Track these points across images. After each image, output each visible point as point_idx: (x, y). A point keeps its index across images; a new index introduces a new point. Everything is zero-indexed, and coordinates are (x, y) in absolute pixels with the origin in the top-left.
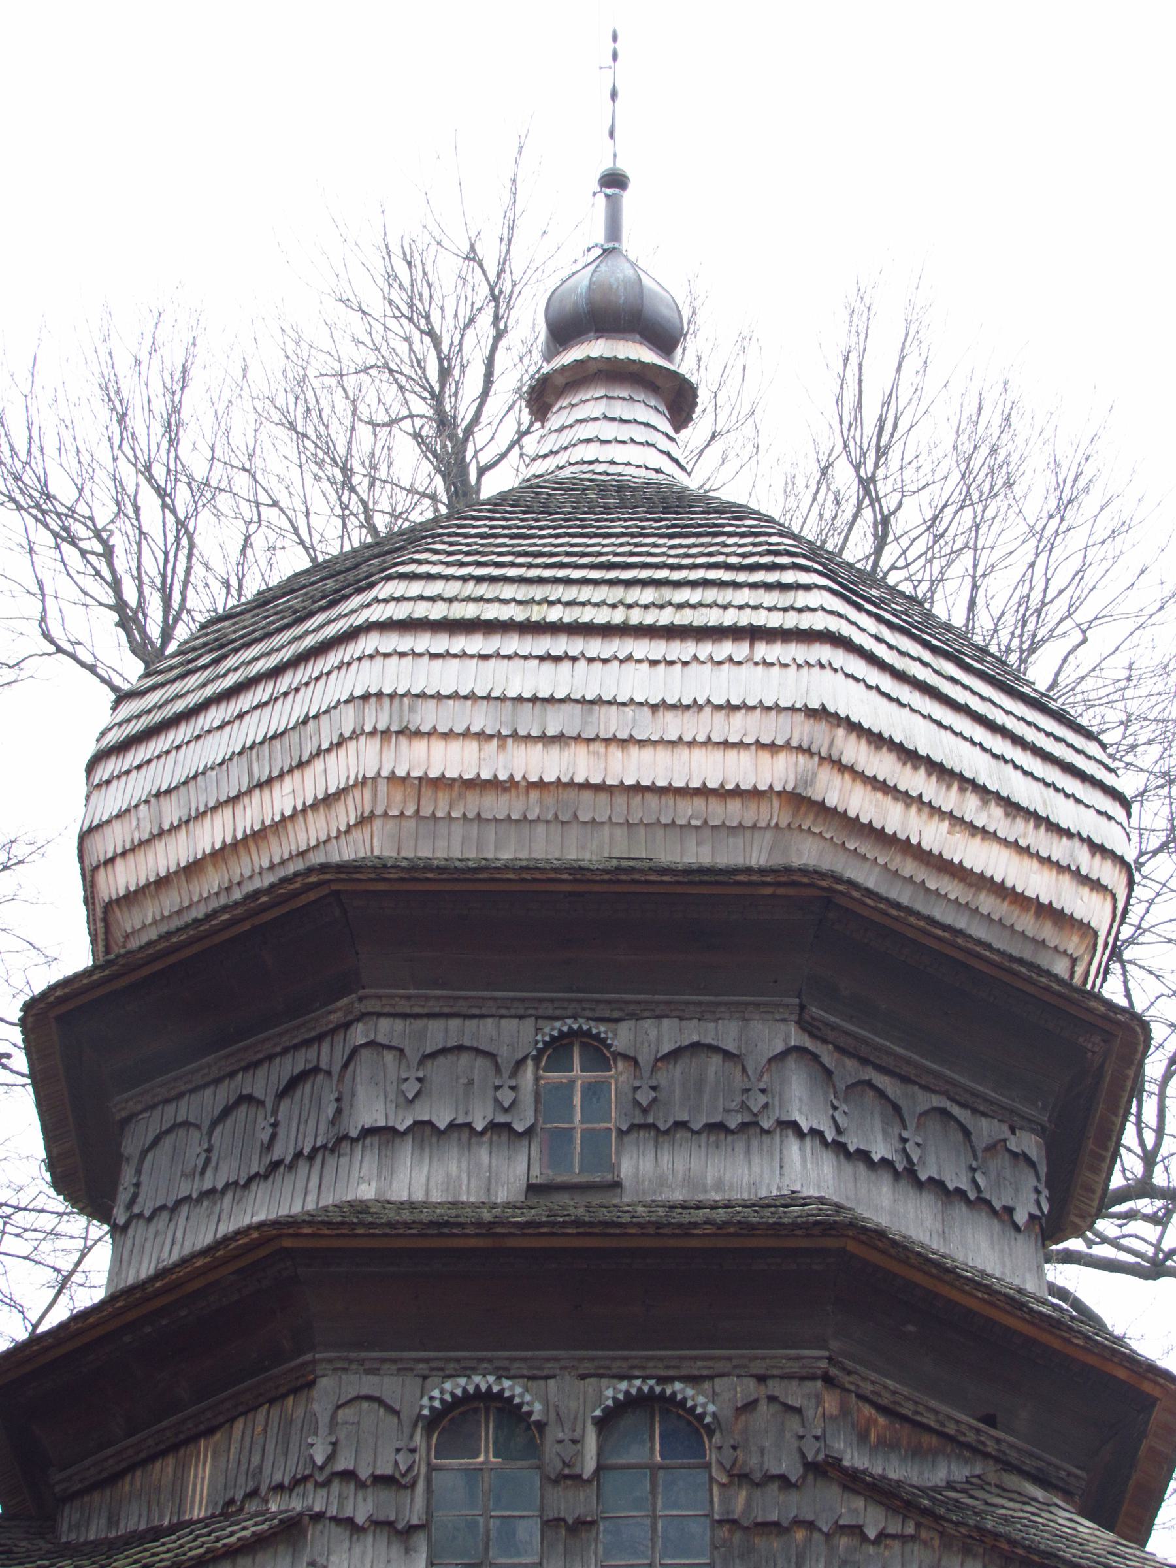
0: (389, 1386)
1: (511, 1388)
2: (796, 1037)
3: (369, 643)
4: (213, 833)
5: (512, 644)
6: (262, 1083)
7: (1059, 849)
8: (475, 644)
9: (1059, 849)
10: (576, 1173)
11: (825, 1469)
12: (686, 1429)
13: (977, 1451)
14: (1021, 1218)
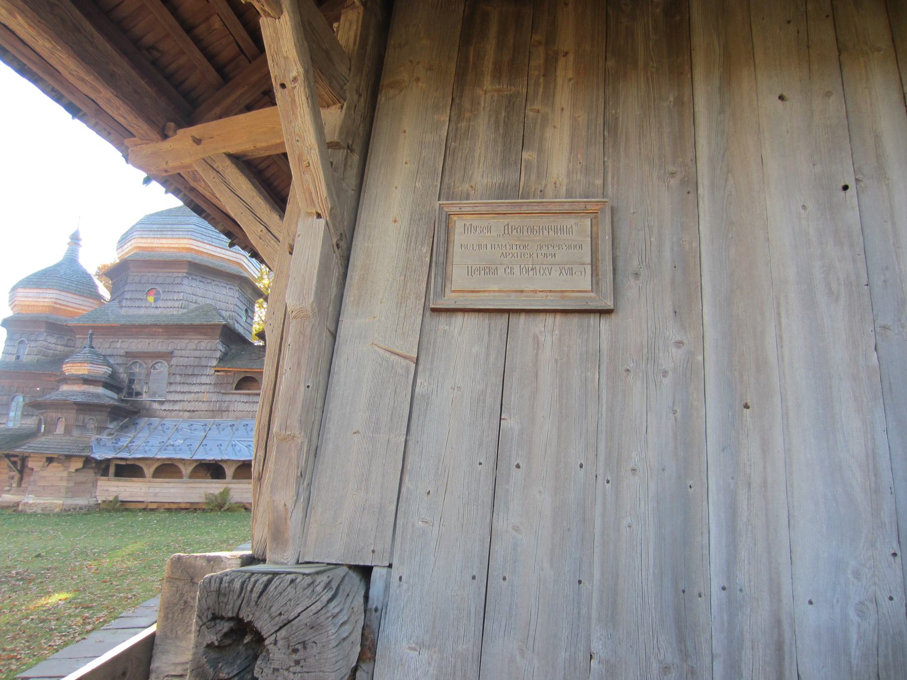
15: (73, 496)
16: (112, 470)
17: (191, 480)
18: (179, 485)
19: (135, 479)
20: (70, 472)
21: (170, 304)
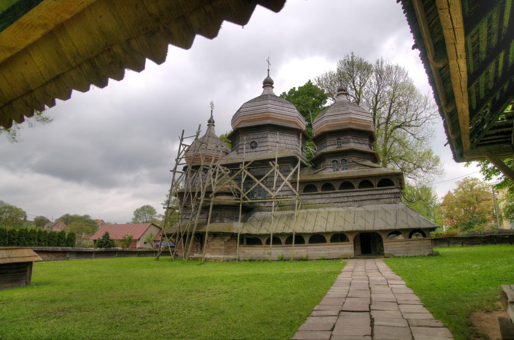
4: (319, 128)
11: (353, 162)
12: (346, 161)
15: (228, 254)
16: (245, 241)
17: (286, 245)
18: (280, 248)
21: (262, 149)
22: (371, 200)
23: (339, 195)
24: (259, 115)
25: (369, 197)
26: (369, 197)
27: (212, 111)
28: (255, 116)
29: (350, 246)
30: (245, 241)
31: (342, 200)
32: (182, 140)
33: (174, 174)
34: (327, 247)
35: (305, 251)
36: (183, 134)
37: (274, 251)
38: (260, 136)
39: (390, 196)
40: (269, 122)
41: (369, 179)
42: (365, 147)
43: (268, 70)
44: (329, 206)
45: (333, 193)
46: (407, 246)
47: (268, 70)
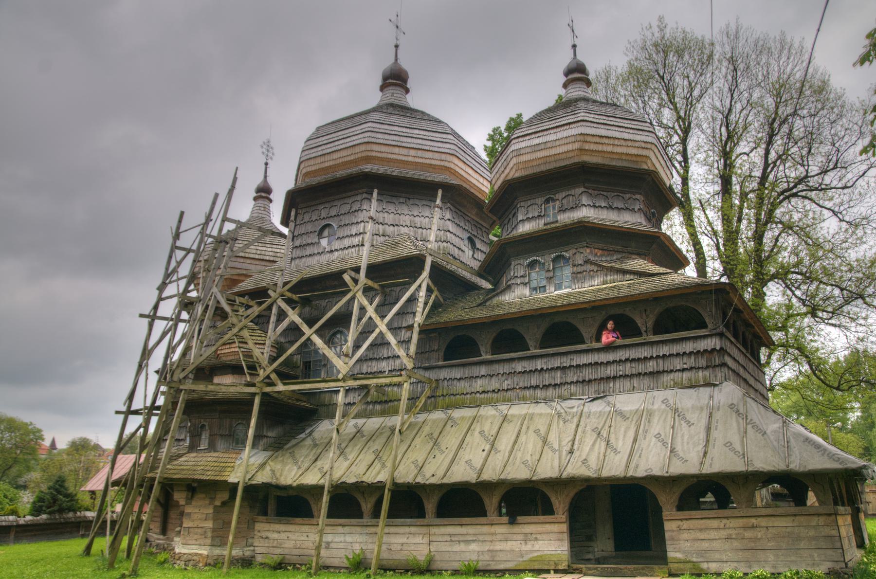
0: (521, 262)
1: (539, 258)
2: (583, 189)
3: (513, 142)
5: (533, 136)
6: (511, 216)
7: (637, 144)
8: (527, 138)
9: (637, 144)
10: (552, 220)
13: (623, 252)
14: (636, 209)
16: (272, 506)
18: (358, 529)
19: (298, 520)
20: (215, 507)
22: (632, 376)
23: (539, 364)
24: (344, 153)
25: (628, 369)
26: (628, 369)
27: (266, 164)
28: (335, 156)
29: (555, 528)
30: (272, 506)
31: (547, 379)
32: (177, 236)
33: (151, 326)
34: (486, 529)
35: (426, 540)
36: (180, 221)
37: (342, 539)
38: (345, 209)
39: (691, 362)
40: (368, 168)
41: (628, 312)
42: (631, 219)
43: (397, 46)
44: (510, 400)
45: (520, 359)
46: (748, 534)
47: (397, 46)
